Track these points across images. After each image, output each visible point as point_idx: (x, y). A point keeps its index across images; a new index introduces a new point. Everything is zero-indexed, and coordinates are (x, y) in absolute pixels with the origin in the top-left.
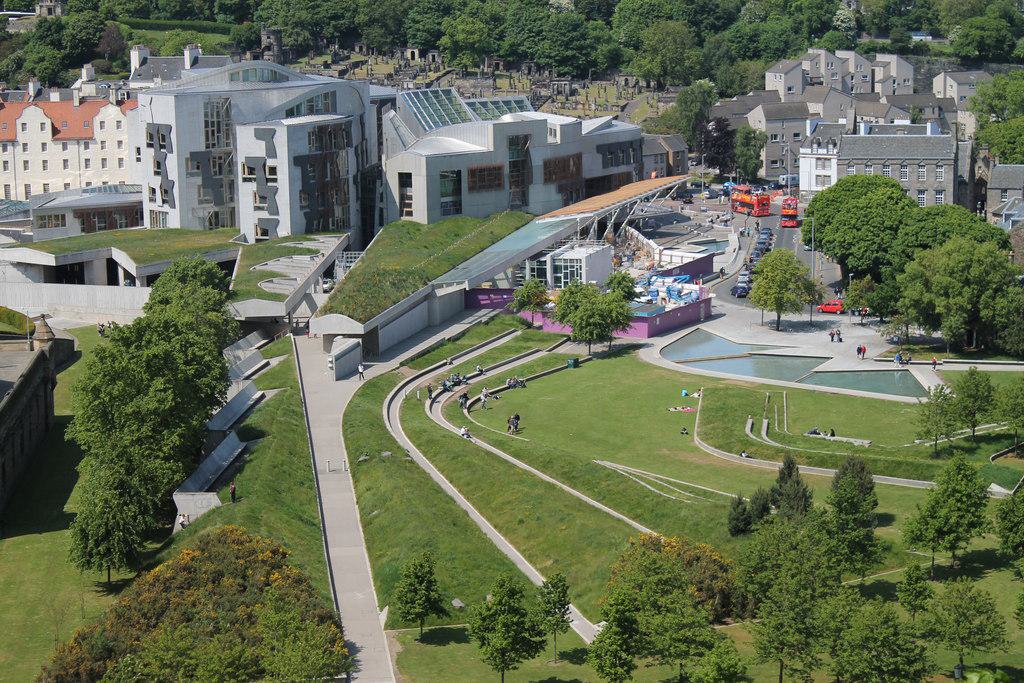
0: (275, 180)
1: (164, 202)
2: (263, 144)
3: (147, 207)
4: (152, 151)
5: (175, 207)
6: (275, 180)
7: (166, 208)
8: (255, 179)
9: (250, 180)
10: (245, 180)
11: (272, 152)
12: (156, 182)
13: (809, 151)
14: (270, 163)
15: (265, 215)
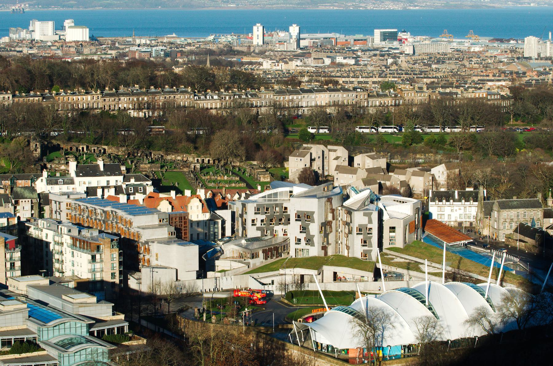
0: (371, 234)
1: (306, 244)
2: (366, 218)
3: (293, 246)
4: (299, 223)
5: (313, 245)
6: (371, 234)
7: (308, 247)
8: (361, 234)
9: (360, 234)
10: (358, 234)
11: (370, 221)
12: (302, 236)
13: (434, 203)
14: (369, 226)
15: (366, 248)
